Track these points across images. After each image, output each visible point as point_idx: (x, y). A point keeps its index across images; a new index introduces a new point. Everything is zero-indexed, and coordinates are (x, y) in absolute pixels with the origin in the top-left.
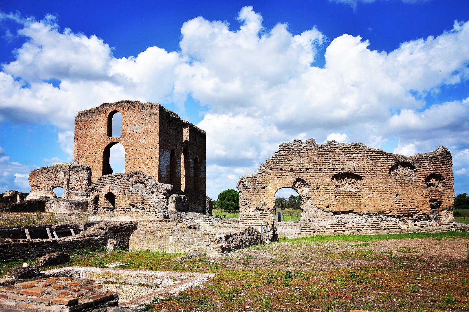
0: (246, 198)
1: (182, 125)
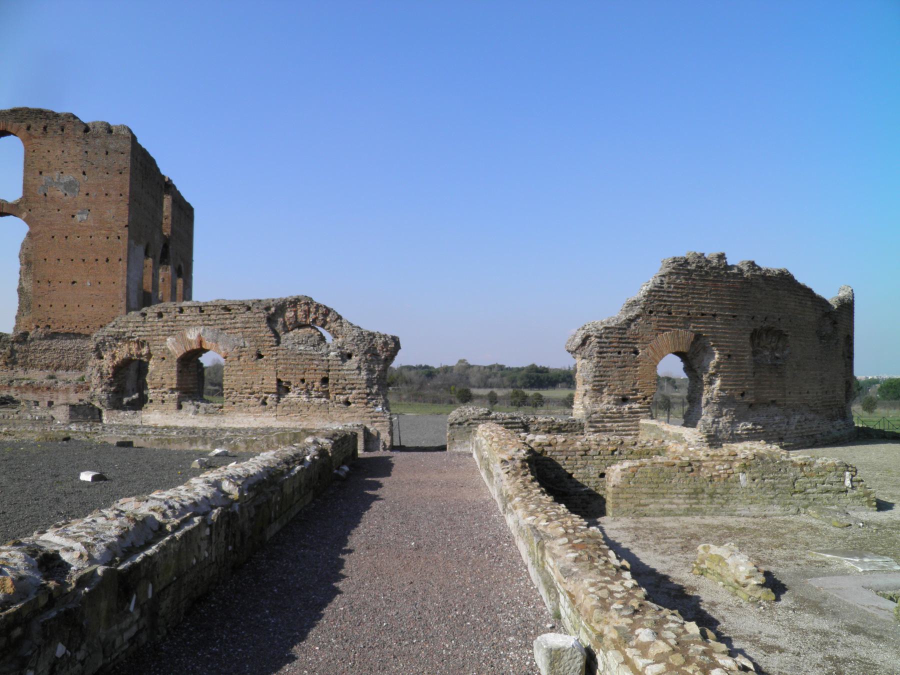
1: (163, 187)
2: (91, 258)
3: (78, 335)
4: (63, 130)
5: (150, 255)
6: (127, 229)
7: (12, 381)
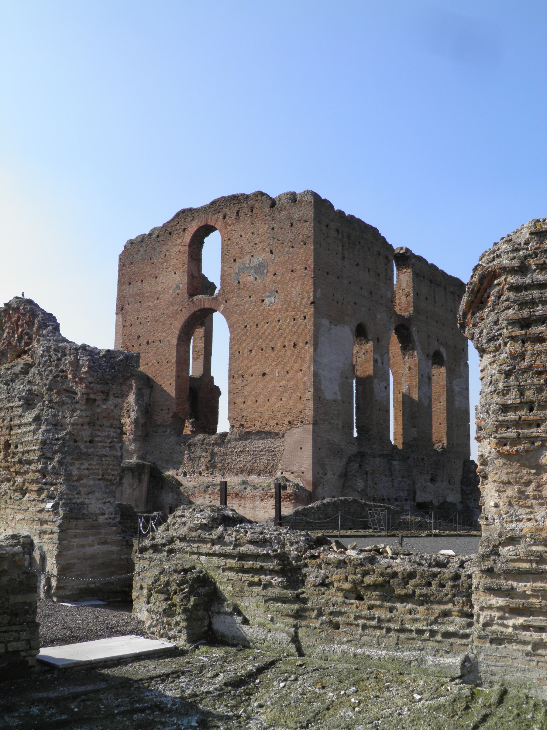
0: (529, 394)
2: (279, 345)
3: (268, 434)
4: (252, 211)
5: (370, 338)
6: (312, 306)
7: (208, 487)
